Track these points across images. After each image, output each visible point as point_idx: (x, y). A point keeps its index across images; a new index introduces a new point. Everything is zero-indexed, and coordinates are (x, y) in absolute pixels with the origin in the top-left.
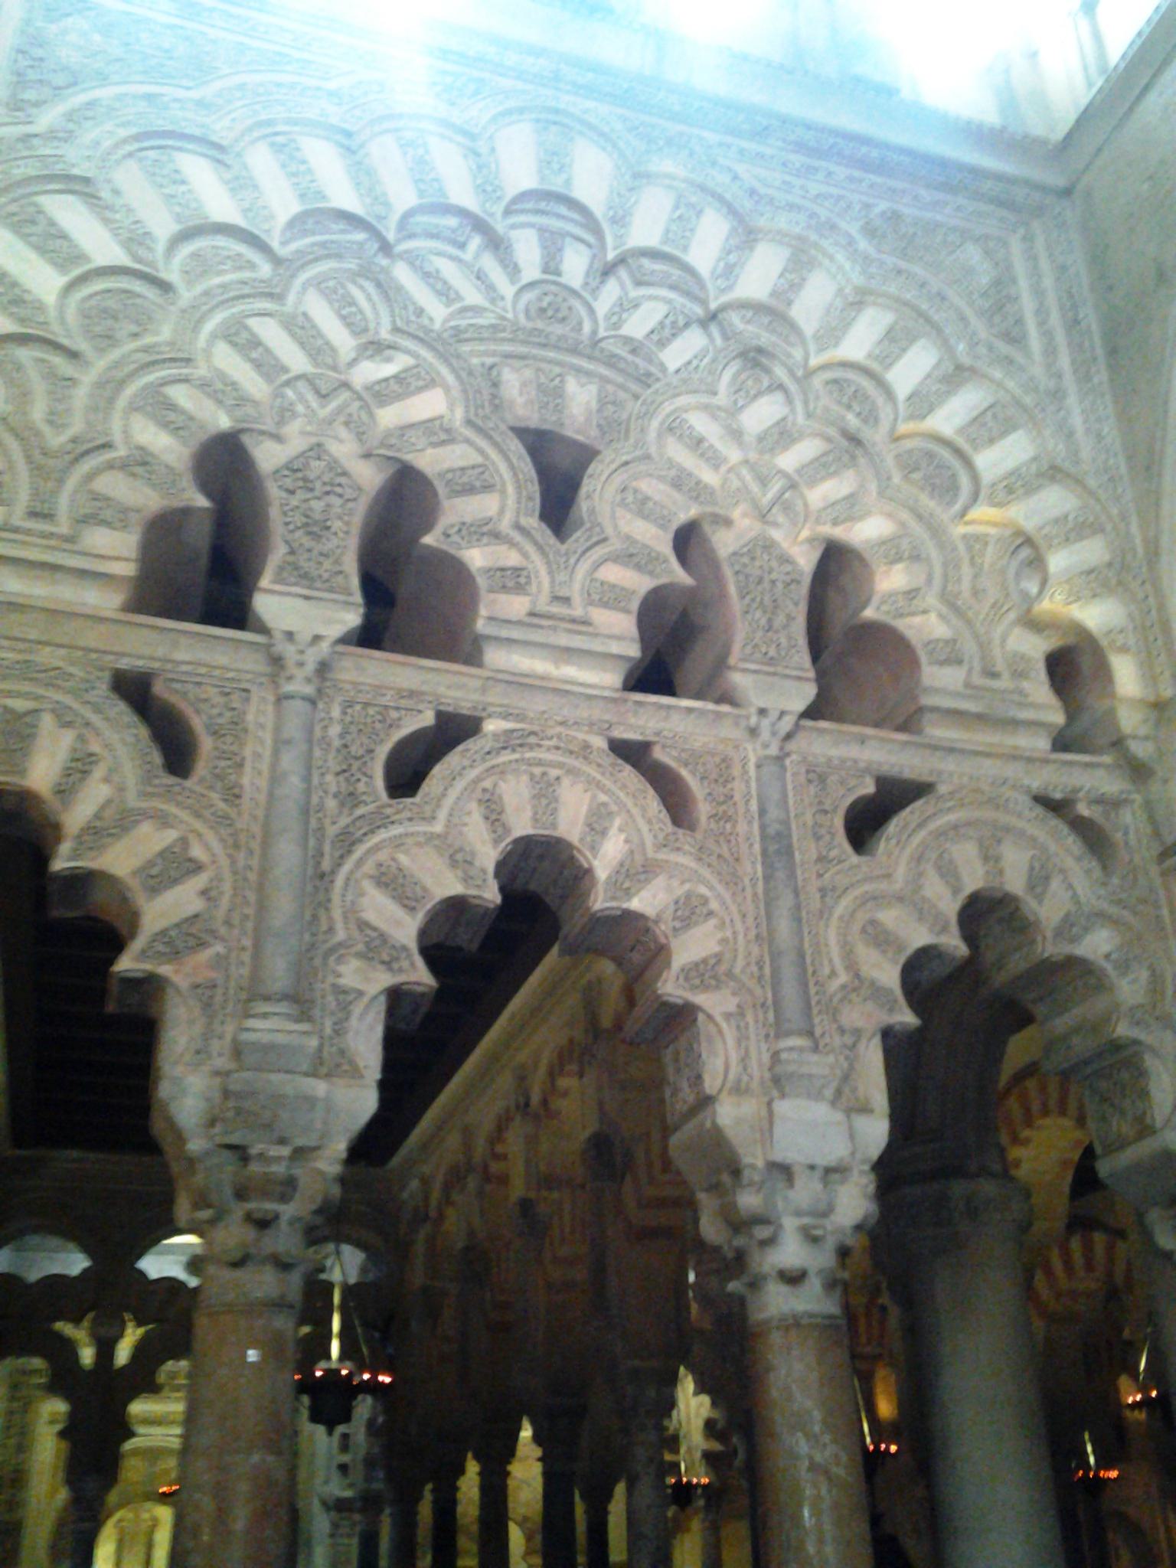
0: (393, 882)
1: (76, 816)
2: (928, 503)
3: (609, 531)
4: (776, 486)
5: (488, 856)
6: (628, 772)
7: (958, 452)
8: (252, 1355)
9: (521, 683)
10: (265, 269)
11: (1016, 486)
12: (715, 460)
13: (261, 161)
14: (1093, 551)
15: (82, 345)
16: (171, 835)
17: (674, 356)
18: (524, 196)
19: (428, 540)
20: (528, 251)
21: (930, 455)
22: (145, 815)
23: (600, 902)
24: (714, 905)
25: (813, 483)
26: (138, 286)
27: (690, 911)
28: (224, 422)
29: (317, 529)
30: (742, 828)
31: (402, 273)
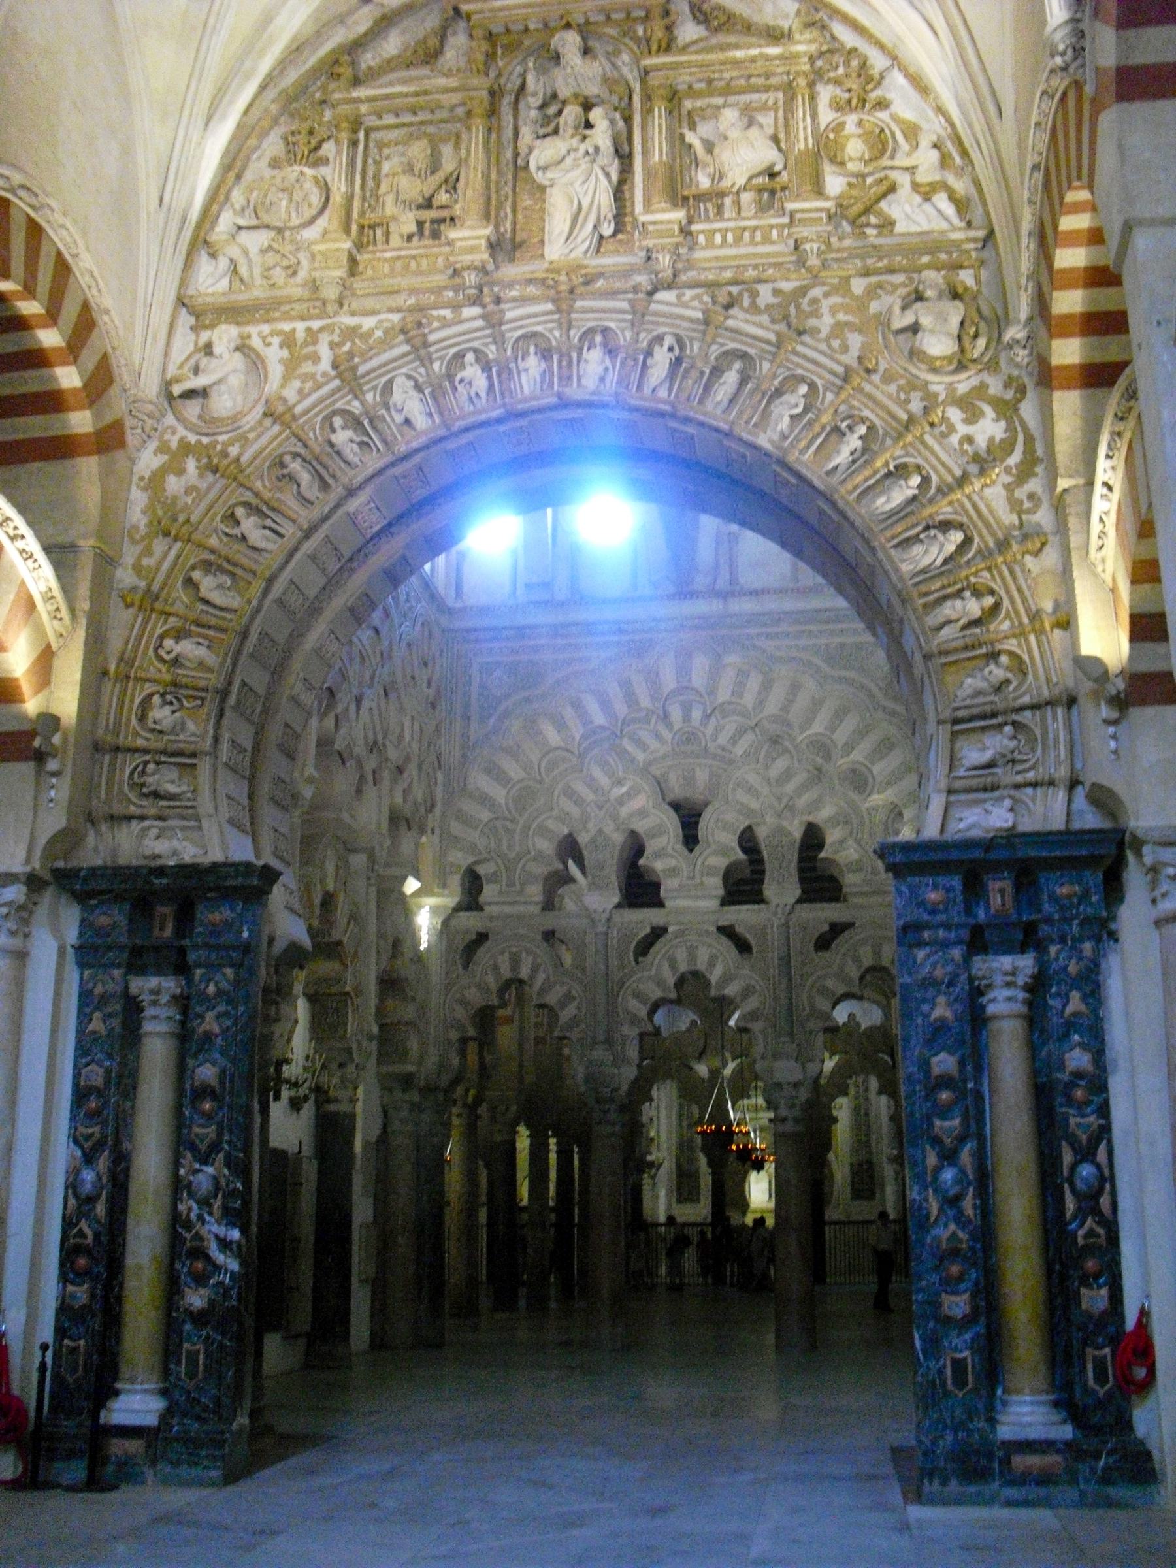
0: (637, 995)
2: (854, 796)
4: (785, 800)
5: (671, 981)
6: (724, 939)
10: (574, 761)
13: (568, 713)
15: (516, 815)
18: (672, 692)
19: (641, 862)
20: (676, 714)
21: (854, 771)
23: (713, 992)
25: (799, 797)
28: (566, 831)
31: (627, 745)
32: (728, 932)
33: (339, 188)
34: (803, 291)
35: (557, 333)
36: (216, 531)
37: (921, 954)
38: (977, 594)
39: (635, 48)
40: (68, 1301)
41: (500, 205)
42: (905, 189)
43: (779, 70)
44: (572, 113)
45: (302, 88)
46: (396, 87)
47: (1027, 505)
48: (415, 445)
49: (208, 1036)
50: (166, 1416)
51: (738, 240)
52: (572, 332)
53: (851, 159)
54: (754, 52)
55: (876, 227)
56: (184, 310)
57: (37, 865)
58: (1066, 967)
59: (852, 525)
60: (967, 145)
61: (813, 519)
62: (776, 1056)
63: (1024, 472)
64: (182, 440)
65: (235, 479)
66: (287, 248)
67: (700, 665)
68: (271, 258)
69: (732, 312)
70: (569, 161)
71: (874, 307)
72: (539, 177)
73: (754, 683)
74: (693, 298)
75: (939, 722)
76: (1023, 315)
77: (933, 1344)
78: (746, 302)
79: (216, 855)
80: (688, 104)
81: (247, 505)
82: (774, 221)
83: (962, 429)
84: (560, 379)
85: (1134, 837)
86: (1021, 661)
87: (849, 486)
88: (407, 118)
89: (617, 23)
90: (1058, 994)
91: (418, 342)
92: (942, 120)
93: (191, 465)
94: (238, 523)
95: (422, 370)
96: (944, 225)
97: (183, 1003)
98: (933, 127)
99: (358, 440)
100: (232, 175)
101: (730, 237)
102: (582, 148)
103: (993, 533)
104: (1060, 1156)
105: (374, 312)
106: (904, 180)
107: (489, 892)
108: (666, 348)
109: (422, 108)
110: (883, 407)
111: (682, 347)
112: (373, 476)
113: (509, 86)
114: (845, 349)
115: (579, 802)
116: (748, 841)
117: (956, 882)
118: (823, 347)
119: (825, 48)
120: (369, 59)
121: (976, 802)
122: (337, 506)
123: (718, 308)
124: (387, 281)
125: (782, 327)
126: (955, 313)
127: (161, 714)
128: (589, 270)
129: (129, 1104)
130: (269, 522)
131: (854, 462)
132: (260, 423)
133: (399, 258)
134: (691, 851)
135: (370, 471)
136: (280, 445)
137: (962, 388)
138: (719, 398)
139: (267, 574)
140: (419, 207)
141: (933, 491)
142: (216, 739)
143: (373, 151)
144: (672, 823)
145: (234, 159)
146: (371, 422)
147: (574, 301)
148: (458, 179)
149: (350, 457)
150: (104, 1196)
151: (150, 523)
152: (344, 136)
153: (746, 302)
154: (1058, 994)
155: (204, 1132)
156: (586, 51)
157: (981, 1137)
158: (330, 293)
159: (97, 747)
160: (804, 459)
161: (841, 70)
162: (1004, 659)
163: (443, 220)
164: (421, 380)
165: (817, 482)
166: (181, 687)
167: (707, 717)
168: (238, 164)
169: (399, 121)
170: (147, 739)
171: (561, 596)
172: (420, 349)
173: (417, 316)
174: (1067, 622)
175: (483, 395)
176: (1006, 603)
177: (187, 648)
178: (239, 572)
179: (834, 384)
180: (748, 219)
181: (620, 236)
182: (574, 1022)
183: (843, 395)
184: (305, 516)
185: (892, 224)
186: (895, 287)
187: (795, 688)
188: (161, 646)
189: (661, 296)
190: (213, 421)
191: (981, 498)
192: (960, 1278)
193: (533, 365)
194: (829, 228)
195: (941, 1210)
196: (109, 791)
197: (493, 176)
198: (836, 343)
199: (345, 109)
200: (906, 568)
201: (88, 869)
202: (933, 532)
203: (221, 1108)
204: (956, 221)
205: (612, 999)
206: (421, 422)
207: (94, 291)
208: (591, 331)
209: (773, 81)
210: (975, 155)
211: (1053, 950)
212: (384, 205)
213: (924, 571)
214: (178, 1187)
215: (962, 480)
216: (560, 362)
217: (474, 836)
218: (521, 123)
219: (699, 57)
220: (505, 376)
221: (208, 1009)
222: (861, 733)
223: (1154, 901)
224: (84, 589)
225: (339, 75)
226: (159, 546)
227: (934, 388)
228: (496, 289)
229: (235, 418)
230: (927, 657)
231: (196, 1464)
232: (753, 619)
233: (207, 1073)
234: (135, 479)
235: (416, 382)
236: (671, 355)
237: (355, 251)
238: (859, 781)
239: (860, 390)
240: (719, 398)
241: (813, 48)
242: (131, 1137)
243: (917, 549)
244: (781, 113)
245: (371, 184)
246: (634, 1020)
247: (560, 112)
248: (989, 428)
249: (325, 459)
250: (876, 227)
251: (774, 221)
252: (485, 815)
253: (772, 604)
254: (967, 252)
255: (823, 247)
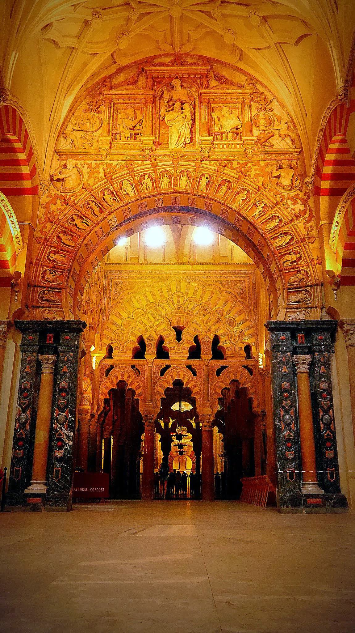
1: (129, 383)
3: (185, 339)
7: (233, 318)
8: (150, 435)
9: (174, 360)
11: (242, 322)
12: (200, 326)
14: (252, 331)
16: (138, 384)
17: (195, 312)
20: (175, 300)
21: (230, 319)
22: (135, 382)
24: (198, 385)
26: (130, 319)
27: (195, 386)
28: (140, 335)
29: (150, 346)
30: (202, 375)
31: (160, 308)
32: (189, 367)
33: (106, 120)
34: (246, 164)
35: (173, 171)
36: (67, 222)
37: (278, 354)
38: (295, 254)
39: (197, 86)
40: (16, 455)
41: (155, 131)
42: (277, 136)
43: (241, 97)
44: (178, 104)
45: (93, 88)
46: (124, 91)
47: (310, 229)
48: (130, 201)
49: (64, 373)
50: (48, 491)
51: (227, 147)
52: (177, 171)
53: (261, 126)
54: (234, 91)
55: (268, 146)
56: (56, 154)
57: (11, 319)
58: (320, 359)
59: (259, 232)
60: (296, 124)
61: (245, 232)
62: (204, 406)
63: (309, 220)
64: (55, 194)
65: (73, 207)
66: (89, 138)
67: (183, 285)
68: (84, 141)
69: (226, 168)
70: (177, 119)
71: (267, 170)
72: (168, 124)
73: (200, 291)
74: (214, 163)
75: (284, 289)
76: (311, 175)
77: (283, 467)
78: (229, 166)
79: (67, 319)
80: (213, 105)
81: (78, 215)
82: (238, 142)
83: (292, 207)
84: (174, 185)
85: (341, 321)
86: (307, 273)
87: (259, 221)
88: (127, 101)
89: (192, 78)
90: (318, 367)
91: (131, 170)
92: (288, 116)
93: (59, 201)
94: (74, 220)
95: (132, 179)
96: (288, 147)
97: (56, 363)
98: (286, 118)
99: (112, 198)
100: (72, 113)
101: (225, 146)
102: (182, 115)
103: (300, 237)
104: (319, 413)
105: (117, 160)
106: (276, 133)
107: (115, 353)
108: (206, 178)
109: (132, 99)
110: (269, 199)
111: (210, 178)
112: (116, 209)
113: (158, 94)
114: (258, 181)
115: (145, 326)
116: (196, 339)
117: (289, 334)
118: (252, 180)
119: (255, 91)
120: (114, 81)
121: (295, 312)
122: (106, 217)
123: (221, 167)
124: (122, 151)
125: (240, 174)
126: (291, 172)
127: (49, 276)
128: (183, 153)
129: (37, 394)
130: (84, 221)
131: (260, 214)
132: (81, 190)
133: (125, 144)
134: (179, 341)
135: (116, 208)
136: (87, 198)
137: (292, 195)
138: (221, 193)
139: (84, 236)
140: (130, 129)
141: (283, 224)
142: (67, 284)
143: (116, 111)
144: (174, 333)
145: (73, 107)
146: (116, 193)
147: (179, 161)
148: (142, 121)
149: (110, 203)
150: (28, 423)
151: (45, 219)
152: (107, 104)
153: (229, 166)
154: (318, 367)
155: (63, 402)
156: (182, 86)
157: (295, 406)
158: (104, 153)
159: (29, 285)
160: (246, 213)
161: (259, 98)
162: (302, 272)
163: (138, 134)
164: (132, 182)
165: (249, 219)
166: (56, 268)
167: (185, 301)
168: (73, 110)
169: (125, 102)
170: (45, 284)
171: (141, 262)
172: (131, 173)
173: (130, 162)
174: (321, 262)
175: (151, 187)
176: (303, 256)
177: (57, 257)
178: (75, 235)
179: (254, 191)
180: (231, 141)
181: (191, 144)
182: (141, 394)
183: (258, 195)
184: (96, 220)
185: (273, 146)
186: (273, 164)
187: (212, 293)
188: (49, 256)
189: (203, 162)
190: (66, 189)
191: (297, 226)
192: (291, 447)
193: (166, 180)
194: (255, 145)
195: (285, 427)
196: (32, 299)
197: (154, 122)
198: (255, 180)
199: (107, 96)
200: (275, 245)
201: (27, 321)
202: (283, 235)
203: (68, 395)
204: (291, 146)
205: (153, 389)
206: (132, 194)
207: (34, 143)
208: (183, 171)
209: (238, 100)
210: (298, 126)
211: (316, 354)
212: (120, 127)
213: (279, 247)
214: (53, 419)
215: (291, 221)
216: (174, 180)
217: (111, 335)
218: (161, 107)
219: (217, 91)
220: (157, 182)
221: (65, 365)
222: (232, 308)
223: (346, 341)
224: (27, 235)
225: (106, 85)
226: (48, 225)
227: (284, 194)
228: (155, 156)
229: (73, 188)
230: (280, 271)
231: (58, 505)
232: (200, 272)
233: (64, 384)
234: (41, 204)
235: (130, 182)
236: (207, 180)
237: (111, 141)
238: (231, 323)
239: (262, 193)
240: (221, 193)
241: (251, 91)
242: (37, 405)
243: (278, 240)
244: (240, 110)
245: (115, 121)
246: (160, 394)
247: (174, 104)
248: (299, 207)
249: (102, 203)
250: (268, 146)
251: (238, 142)
252: (115, 328)
253: (206, 267)
254: (294, 155)
255: (253, 151)
